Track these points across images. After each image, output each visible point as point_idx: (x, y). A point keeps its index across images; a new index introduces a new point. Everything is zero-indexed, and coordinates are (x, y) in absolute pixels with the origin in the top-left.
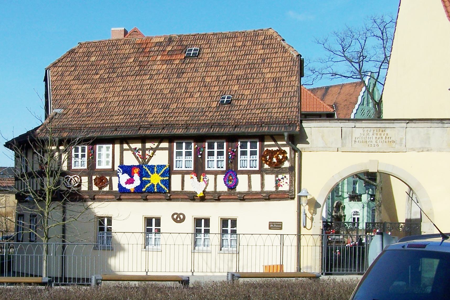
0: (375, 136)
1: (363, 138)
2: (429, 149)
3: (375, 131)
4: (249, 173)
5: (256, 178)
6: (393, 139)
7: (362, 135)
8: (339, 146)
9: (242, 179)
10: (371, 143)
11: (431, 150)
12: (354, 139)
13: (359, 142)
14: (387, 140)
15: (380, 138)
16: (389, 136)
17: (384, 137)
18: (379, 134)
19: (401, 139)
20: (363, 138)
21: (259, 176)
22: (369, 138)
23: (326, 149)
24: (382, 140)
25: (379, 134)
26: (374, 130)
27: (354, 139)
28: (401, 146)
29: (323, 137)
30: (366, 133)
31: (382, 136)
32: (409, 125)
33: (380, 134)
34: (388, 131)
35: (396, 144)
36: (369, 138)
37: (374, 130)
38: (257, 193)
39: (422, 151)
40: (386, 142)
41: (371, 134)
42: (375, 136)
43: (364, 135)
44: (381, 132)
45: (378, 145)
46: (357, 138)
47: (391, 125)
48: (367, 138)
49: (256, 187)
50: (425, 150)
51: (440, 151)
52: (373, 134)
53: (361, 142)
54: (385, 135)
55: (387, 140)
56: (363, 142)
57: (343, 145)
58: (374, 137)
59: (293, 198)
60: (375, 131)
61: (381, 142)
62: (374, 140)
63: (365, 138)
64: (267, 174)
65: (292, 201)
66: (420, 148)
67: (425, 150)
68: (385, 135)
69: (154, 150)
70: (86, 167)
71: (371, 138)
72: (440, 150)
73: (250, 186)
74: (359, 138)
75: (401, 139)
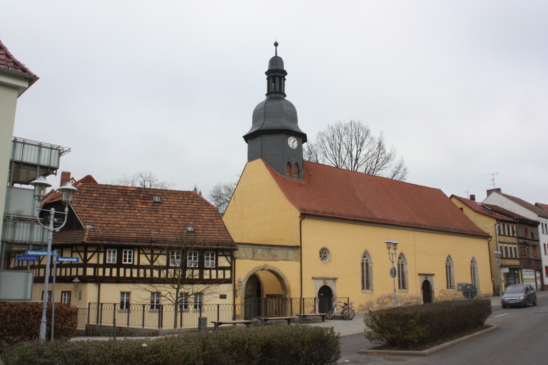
4: (210, 269)
5: (214, 272)
6: (274, 254)
8: (252, 257)
9: (207, 272)
23: (246, 258)
29: (245, 252)
38: (214, 280)
39: (286, 261)
41: (265, 251)
42: (267, 253)
47: (274, 248)
49: (214, 277)
57: (253, 256)
59: (231, 283)
62: (266, 255)
69: (158, 255)
70: (116, 262)
72: (292, 260)
73: (211, 276)
75: (278, 255)
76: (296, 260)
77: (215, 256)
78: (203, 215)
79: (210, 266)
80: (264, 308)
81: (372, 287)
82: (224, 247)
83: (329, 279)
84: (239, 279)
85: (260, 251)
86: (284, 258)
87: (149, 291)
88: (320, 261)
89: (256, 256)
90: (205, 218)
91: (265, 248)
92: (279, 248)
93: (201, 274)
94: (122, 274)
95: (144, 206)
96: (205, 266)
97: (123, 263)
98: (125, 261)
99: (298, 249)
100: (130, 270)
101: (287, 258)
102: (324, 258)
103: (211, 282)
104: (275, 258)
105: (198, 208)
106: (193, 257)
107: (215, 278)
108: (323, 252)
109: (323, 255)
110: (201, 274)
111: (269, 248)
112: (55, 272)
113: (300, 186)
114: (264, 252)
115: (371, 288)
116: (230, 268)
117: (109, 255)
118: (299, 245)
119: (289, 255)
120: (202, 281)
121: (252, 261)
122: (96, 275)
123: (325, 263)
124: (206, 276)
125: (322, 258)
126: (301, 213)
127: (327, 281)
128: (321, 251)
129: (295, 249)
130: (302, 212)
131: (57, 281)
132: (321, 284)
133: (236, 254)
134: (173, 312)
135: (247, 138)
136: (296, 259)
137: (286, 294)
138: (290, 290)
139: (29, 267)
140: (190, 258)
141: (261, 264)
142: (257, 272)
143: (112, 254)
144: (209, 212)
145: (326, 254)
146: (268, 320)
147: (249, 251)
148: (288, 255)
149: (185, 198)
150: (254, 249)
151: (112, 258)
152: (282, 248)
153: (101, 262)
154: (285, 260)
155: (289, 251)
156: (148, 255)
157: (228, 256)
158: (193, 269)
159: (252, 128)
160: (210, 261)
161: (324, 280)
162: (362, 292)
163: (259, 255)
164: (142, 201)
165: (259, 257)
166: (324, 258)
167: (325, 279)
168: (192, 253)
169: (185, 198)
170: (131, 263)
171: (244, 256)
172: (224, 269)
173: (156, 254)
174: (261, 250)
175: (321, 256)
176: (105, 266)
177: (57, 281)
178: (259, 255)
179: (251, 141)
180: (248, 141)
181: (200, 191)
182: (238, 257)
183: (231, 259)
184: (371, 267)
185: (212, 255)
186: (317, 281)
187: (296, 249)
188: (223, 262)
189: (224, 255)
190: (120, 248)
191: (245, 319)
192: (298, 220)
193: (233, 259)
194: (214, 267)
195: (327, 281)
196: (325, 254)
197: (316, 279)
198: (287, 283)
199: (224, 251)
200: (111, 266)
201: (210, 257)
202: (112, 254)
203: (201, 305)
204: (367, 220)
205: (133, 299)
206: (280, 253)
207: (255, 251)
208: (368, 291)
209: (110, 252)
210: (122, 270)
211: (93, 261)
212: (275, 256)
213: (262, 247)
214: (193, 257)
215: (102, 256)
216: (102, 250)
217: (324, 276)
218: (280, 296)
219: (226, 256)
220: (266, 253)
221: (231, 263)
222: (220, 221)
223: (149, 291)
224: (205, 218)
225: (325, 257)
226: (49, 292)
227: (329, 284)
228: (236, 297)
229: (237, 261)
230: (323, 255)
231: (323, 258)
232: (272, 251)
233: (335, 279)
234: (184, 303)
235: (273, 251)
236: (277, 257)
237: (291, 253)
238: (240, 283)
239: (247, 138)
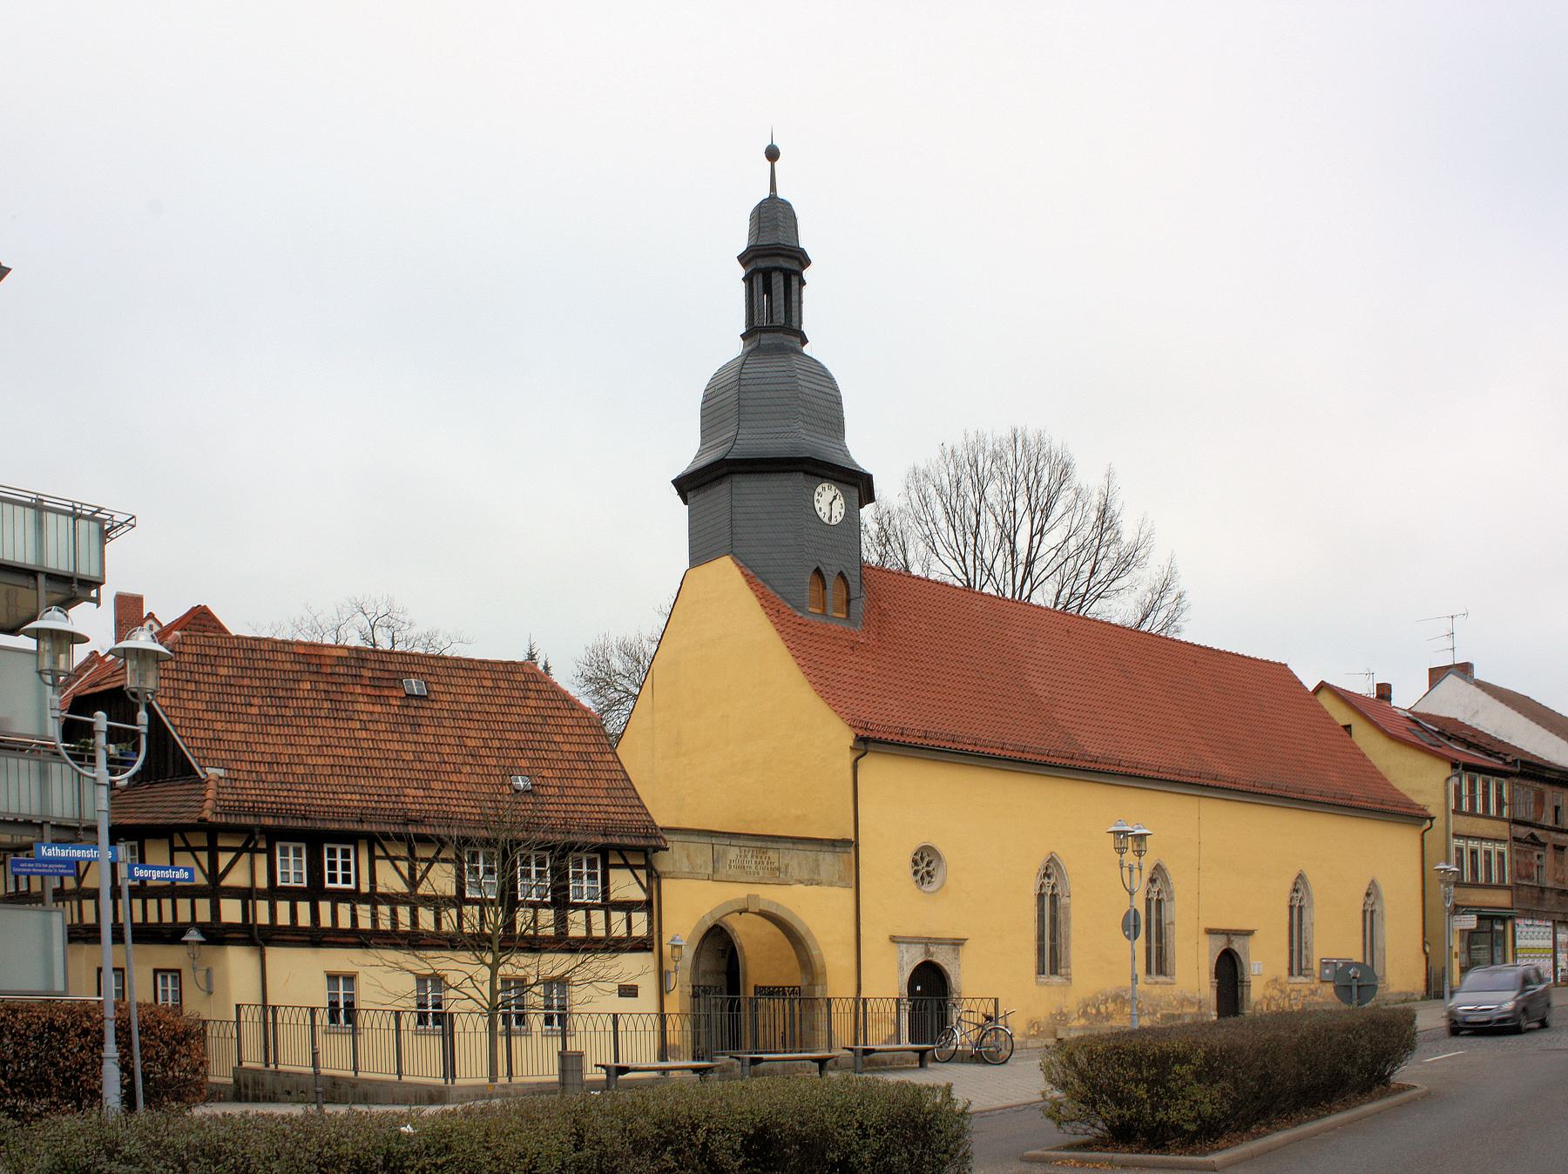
3: (755, 852)
4: (588, 908)
5: (598, 916)
6: (776, 865)
9: (577, 917)
11: (822, 883)
21: (601, 913)
23: (693, 875)
27: (728, 862)
29: (688, 856)
33: (761, 857)
38: (599, 940)
39: (811, 884)
45: (758, 873)
47: (775, 846)
50: (814, 883)
59: (651, 950)
60: (755, 852)
62: (753, 866)
64: (615, 910)
65: (650, 954)
67: (814, 883)
69: (431, 862)
70: (305, 884)
72: (831, 884)
75: (787, 866)
76: (840, 882)
77: (599, 867)
78: (557, 739)
79: (586, 897)
80: (748, 1027)
81: (1068, 967)
82: (626, 841)
83: (939, 942)
84: (673, 940)
85: (733, 853)
86: (806, 877)
87: (411, 972)
88: (914, 886)
89: (724, 871)
90: (566, 748)
91: (750, 843)
92: (789, 845)
93: (561, 922)
94: (325, 921)
95: (378, 708)
96: (571, 899)
97: (328, 885)
98: (333, 879)
99: (848, 850)
100: (348, 906)
102: (927, 879)
103: (589, 945)
104: (779, 877)
105: (544, 717)
106: (534, 869)
107: (602, 934)
108: (922, 858)
109: (922, 867)
110: (561, 922)
111: (759, 844)
112: (129, 912)
113: (852, 648)
115: (1063, 971)
116: (647, 906)
117: (285, 862)
118: (851, 836)
119: (822, 868)
120: (563, 943)
121: (710, 883)
122: (251, 922)
123: (928, 892)
124: (576, 931)
125: (919, 877)
126: (857, 735)
127: (933, 949)
128: (918, 857)
129: (838, 850)
130: (860, 733)
131: (136, 940)
132: (915, 957)
133: (663, 862)
134: (483, 1035)
135: (687, 485)
137: (812, 984)
138: (824, 974)
139: (49, 895)
140: (526, 874)
141: (738, 892)
142: (725, 918)
143: (291, 857)
144: (577, 731)
145: (933, 865)
146: (761, 1060)
147: (701, 852)
148: (818, 866)
149: (502, 684)
150: (716, 847)
151: (292, 869)
152: (801, 847)
153: (262, 882)
154: (810, 882)
155: (821, 856)
156: (398, 863)
157: (639, 867)
158: (535, 906)
159: (701, 453)
160: (586, 884)
161: (926, 944)
162: (1037, 982)
163: (730, 867)
164: (369, 690)
165: (730, 872)
166: (927, 879)
167: (927, 942)
168: (529, 857)
169: (502, 684)
170: (352, 886)
171: (687, 870)
172: (628, 907)
173: (422, 860)
175: (916, 873)
176: (274, 893)
177: (136, 940)
178: (730, 867)
179: (697, 498)
180: (689, 495)
181: (546, 663)
182: (670, 872)
183: (649, 876)
184: (1067, 907)
185: (592, 864)
186: (903, 947)
187: (842, 849)
188: (625, 885)
189: (626, 865)
190: (314, 841)
191: (694, 1059)
192: (848, 758)
193: (654, 877)
194: (599, 901)
195: (933, 949)
196: (928, 865)
197: (903, 942)
198: (815, 952)
199: (625, 853)
200: (293, 895)
201: (585, 869)
202: (291, 857)
203: (565, 1015)
204: (1059, 761)
205: (366, 996)
206: (795, 860)
207: (718, 853)
208: (1056, 979)
209: (285, 852)
210: (325, 907)
211: (237, 878)
212: (779, 869)
213: (741, 843)
214: (534, 869)
215: (261, 862)
216: (262, 845)
217: (925, 933)
218: (795, 990)
219: (632, 868)
220: (751, 861)
221: (648, 890)
222: (610, 757)
223: (411, 972)
224: (566, 748)
225: (928, 873)
226: (115, 969)
227: (941, 957)
228: (667, 993)
229: (665, 883)
230: (922, 867)
231: (922, 878)
232: (770, 853)
233: (957, 943)
234: (513, 1008)
237: (829, 862)
238: (676, 950)
239: (687, 485)
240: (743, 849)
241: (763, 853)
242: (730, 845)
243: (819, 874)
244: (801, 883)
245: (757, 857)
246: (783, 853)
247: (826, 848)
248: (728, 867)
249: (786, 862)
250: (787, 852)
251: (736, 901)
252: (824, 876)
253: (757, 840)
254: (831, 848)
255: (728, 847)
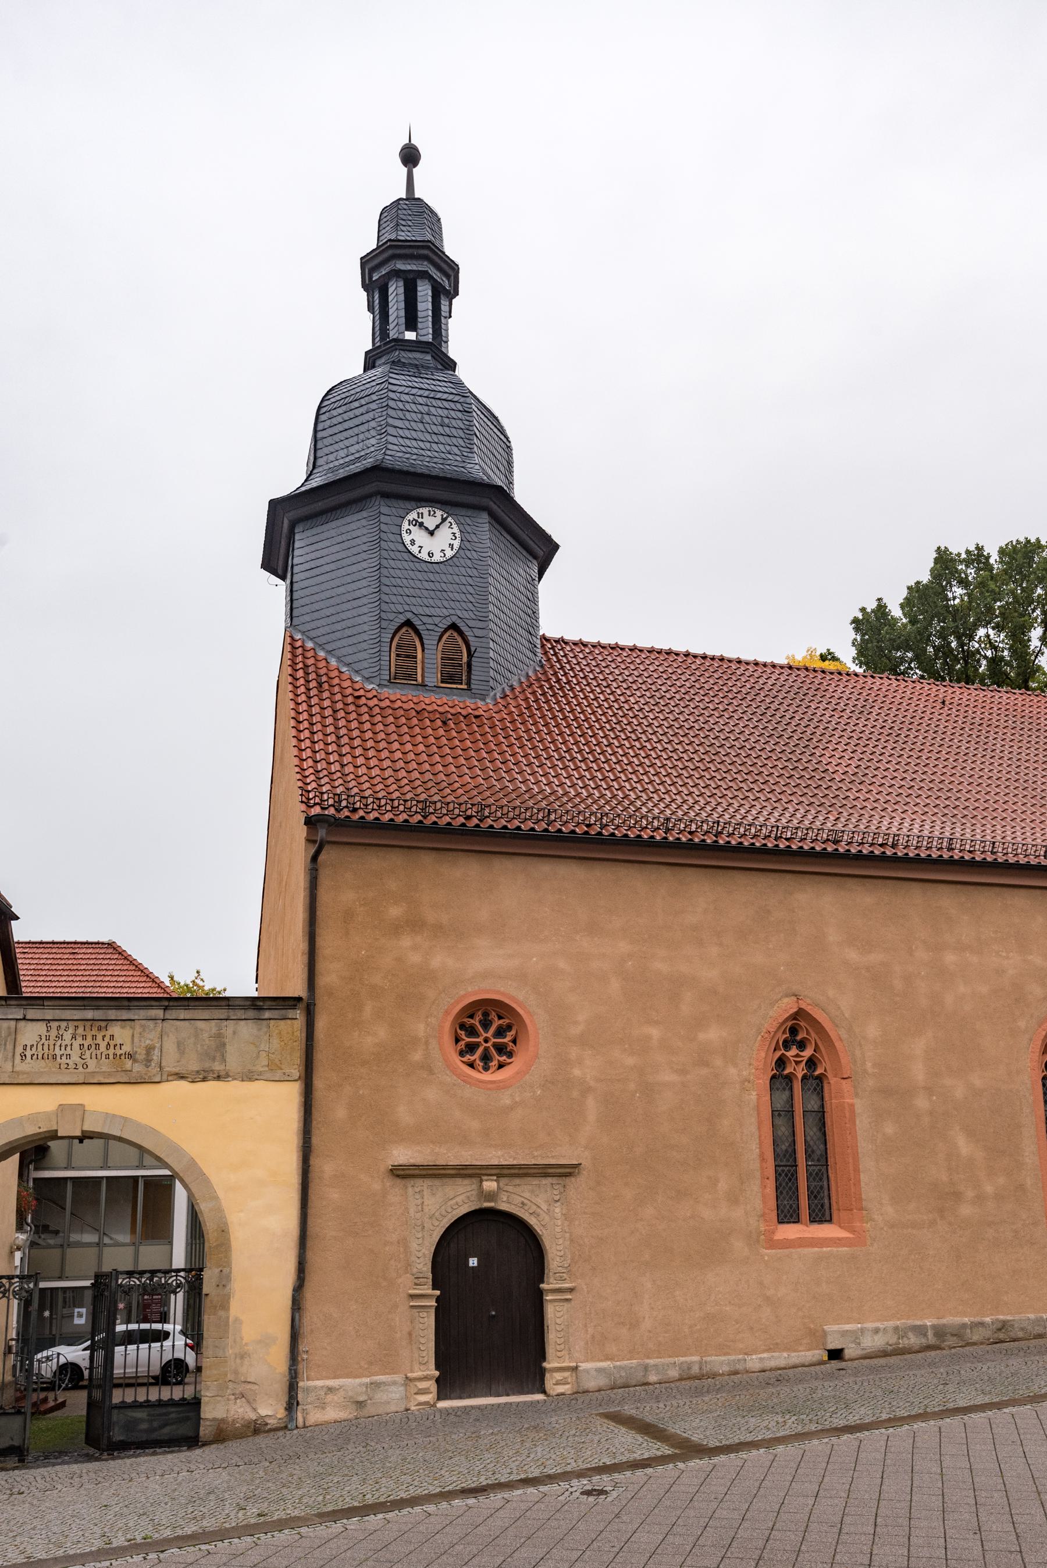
0: (80, 1041)
1: (46, 1047)
2: (222, 1073)
3: (80, 1031)
6: (127, 1048)
7: (44, 1038)
10: (68, 1061)
11: (227, 1075)
12: (19, 1050)
13: (35, 1056)
14: (111, 1051)
15: (93, 1046)
16: (118, 1040)
17: (103, 1045)
18: (89, 1038)
19: (149, 1050)
20: (46, 1047)
22: (63, 1048)
24: (99, 1053)
25: (89, 1038)
26: (76, 1027)
27: (19, 1050)
28: (148, 1067)
30: (53, 1033)
31: (99, 1040)
32: (172, 1014)
33: (94, 1037)
34: (116, 1030)
35: (135, 1061)
36: (63, 1048)
37: (76, 1027)
39: (204, 1080)
40: (107, 1057)
41: (67, 1036)
42: (80, 1041)
43: (48, 1038)
44: (94, 1033)
45: (85, 1066)
46: (28, 1048)
47: (125, 1015)
48: (57, 1048)
51: (250, 1080)
52: (74, 1037)
53: (40, 1056)
54: (107, 1039)
55: (111, 1051)
56: (46, 1056)
58: (76, 1045)
60: (80, 1031)
61: (94, 1056)
63: (52, 1047)
66: (198, 1072)
68: (107, 1039)
71: (69, 1048)
72: (249, 1077)
74: (34, 1049)
75: (149, 1050)
76: (273, 1073)
86: (194, 1066)
92: (159, 1013)
99: (291, 1013)
101: (217, 1066)
111: (89, 1014)
114: (60, 1037)
119: (231, 1050)
129: (267, 1014)
136: (272, 1066)
148: (224, 1045)
152: (182, 1014)
155: (229, 1027)
163: (23, 1056)
165: (20, 1066)
174: (41, 1028)
178: (23, 1056)
212: (130, 1056)
213: (49, 1014)
235: (120, 1033)
236: (148, 1061)
240: (54, 1025)
241: (100, 1029)
242: (24, 1019)
243: (224, 1060)
244: (183, 1078)
245: (84, 1037)
246: (143, 1027)
247: (240, 1014)
248: (18, 1058)
249: (148, 1042)
250: (151, 1024)
251: (32, 1118)
252: (233, 1062)
253: (85, 1007)
254: (251, 1013)
255: (22, 1024)
